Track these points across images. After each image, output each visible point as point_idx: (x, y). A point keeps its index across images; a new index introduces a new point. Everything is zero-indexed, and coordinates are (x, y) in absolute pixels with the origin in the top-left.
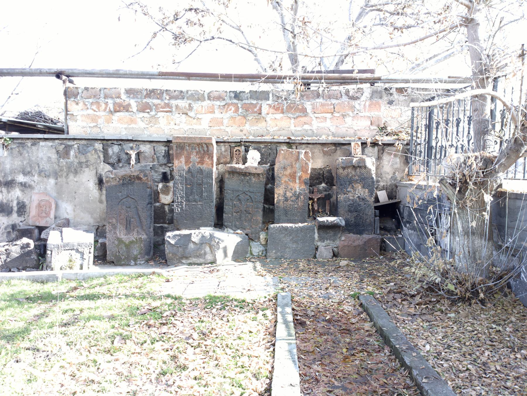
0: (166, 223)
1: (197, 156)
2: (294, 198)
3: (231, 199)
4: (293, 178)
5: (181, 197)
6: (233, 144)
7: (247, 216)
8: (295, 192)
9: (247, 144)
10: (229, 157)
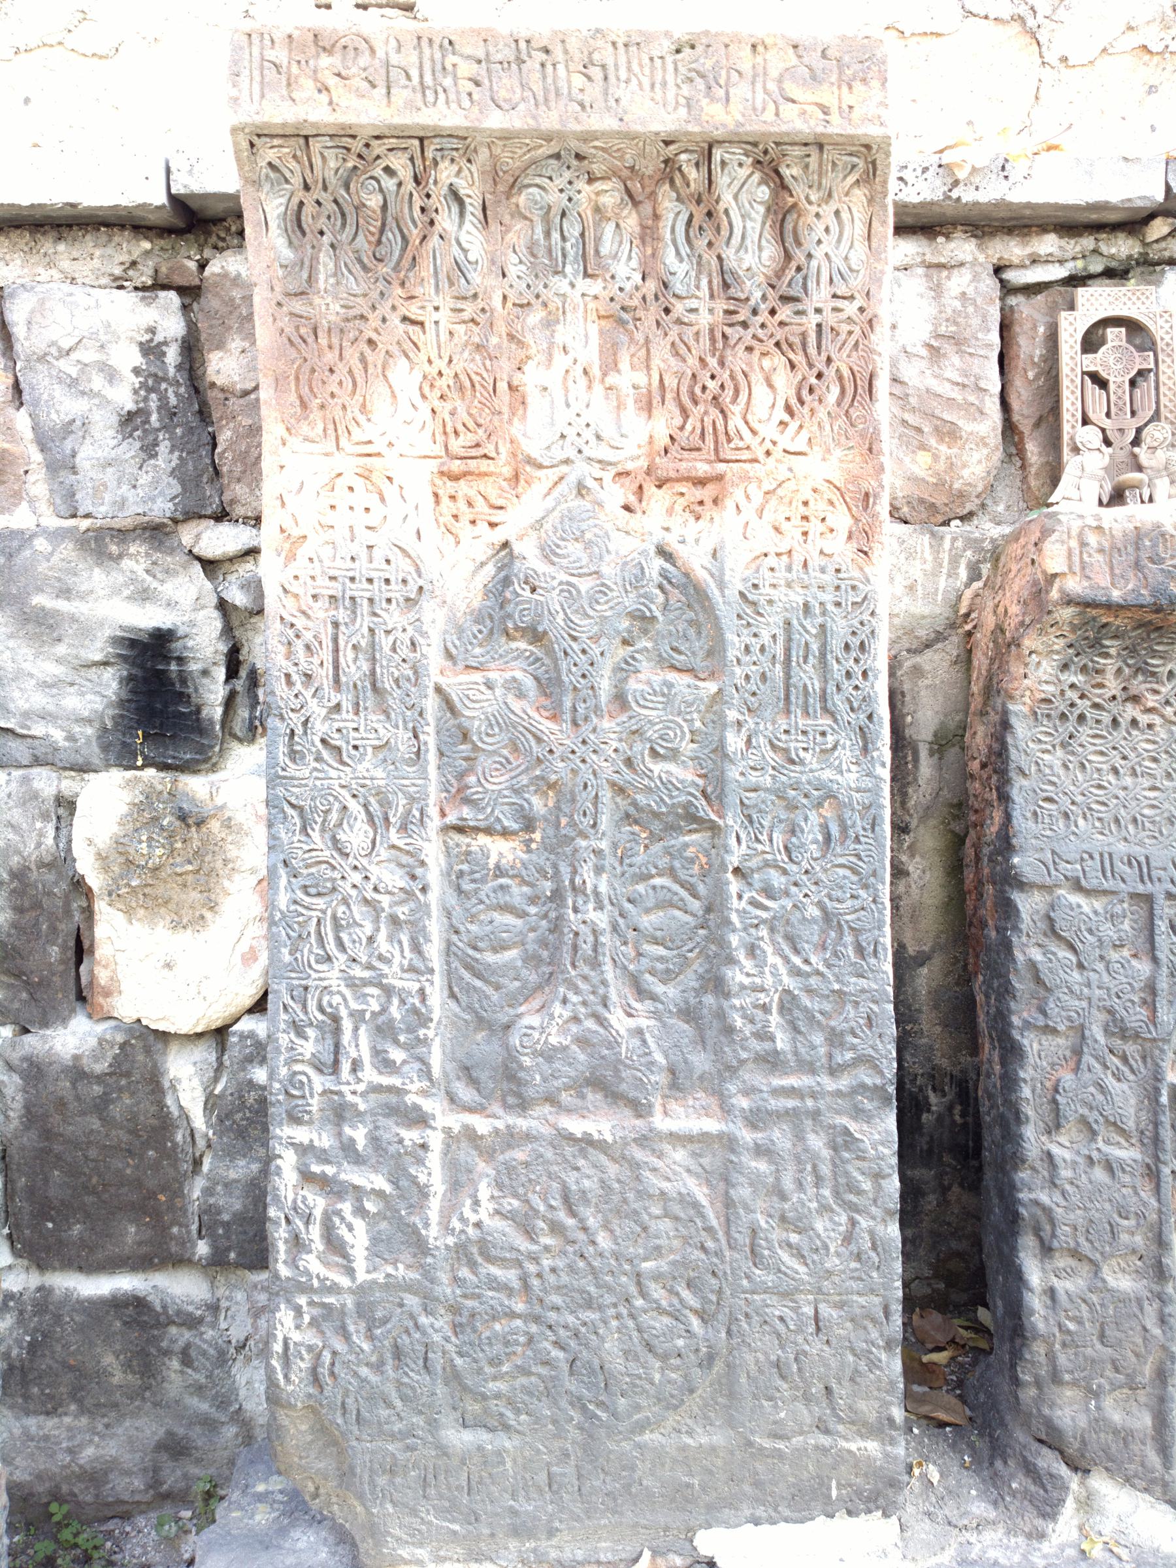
0: (179, 1261)
1: (629, 377)
3: (1118, 1029)
5: (385, 1030)
6: (1049, 244)
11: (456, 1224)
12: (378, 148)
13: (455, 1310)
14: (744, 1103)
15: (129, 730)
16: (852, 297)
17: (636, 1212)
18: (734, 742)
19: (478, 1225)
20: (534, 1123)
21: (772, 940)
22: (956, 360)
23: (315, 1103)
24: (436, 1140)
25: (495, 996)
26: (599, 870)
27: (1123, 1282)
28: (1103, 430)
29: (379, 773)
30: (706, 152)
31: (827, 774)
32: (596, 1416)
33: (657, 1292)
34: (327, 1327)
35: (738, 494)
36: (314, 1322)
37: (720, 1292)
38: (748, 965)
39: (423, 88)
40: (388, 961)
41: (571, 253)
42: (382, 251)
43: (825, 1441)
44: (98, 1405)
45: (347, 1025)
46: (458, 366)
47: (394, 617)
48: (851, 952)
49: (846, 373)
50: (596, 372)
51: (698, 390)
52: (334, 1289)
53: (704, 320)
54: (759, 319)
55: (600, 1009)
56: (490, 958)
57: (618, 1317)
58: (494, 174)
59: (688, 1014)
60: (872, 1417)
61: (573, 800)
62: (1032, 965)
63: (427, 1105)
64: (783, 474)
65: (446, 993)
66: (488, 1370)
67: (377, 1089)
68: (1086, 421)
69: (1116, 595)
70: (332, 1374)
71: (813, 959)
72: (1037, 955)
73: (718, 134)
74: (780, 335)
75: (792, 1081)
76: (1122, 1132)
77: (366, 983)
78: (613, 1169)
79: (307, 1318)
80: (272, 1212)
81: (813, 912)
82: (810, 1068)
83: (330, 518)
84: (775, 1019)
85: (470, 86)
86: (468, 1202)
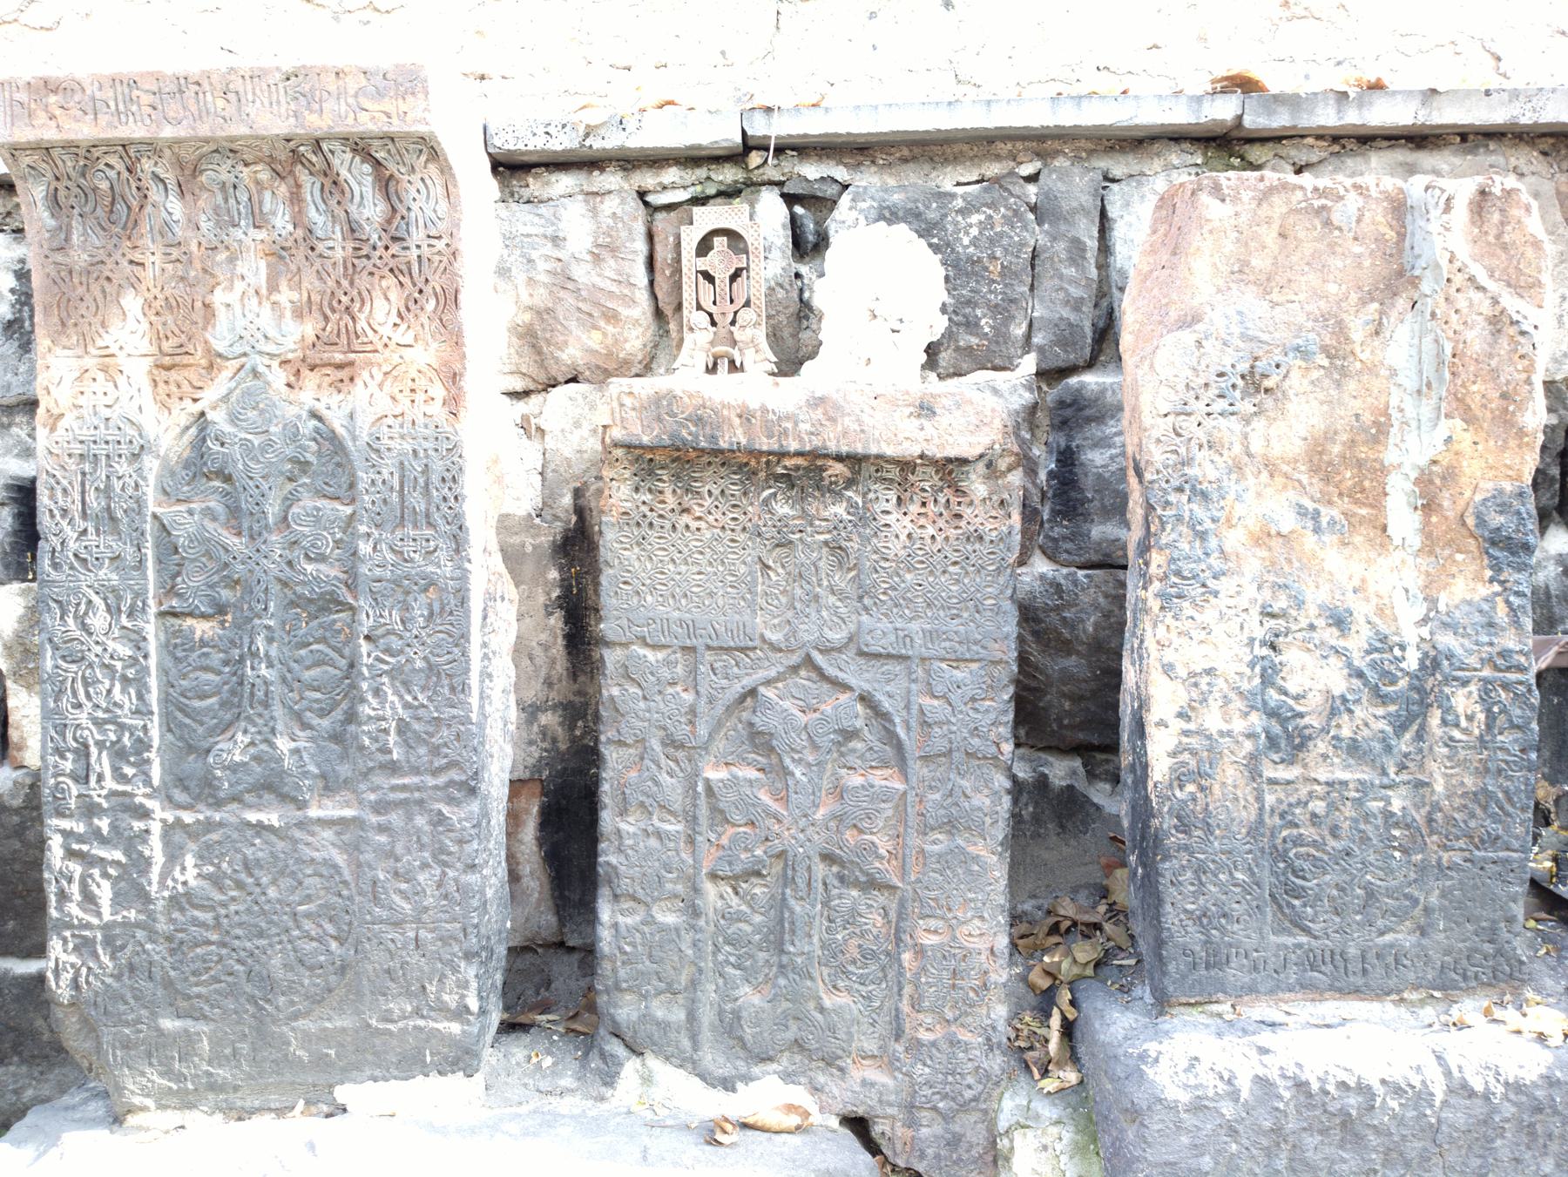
1: (286, 296)
2: (1369, 719)
3: (671, 742)
4: (1357, 494)
5: (119, 754)
6: (671, 175)
7: (852, 917)
8: (1382, 643)
9: (812, 171)
10: (641, 308)
11: (170, 883)
12: (96, 153)
13: (169, 939)
14: (372, 797)
15: (22, 553)
16: (439, 238)
17: (293, 873)
18: (365, 548)
19: (185, 883)
20: (225, 815)
21: (393, 685)
22: (612, 262)
23: (73, 803)
24: (156, 828)
25: (200, 730)
26: (270, 640)
27: (668, 917)
28: (710, 315)
29: (114, 576)
30: (317, 144)
31: (431, 569)
32: (263, 1008)
33: (308, 925)
34: (84, 950)
35: (365, 374)
36: (76, 948)
37: (350, 924)
38: (374, 702)
39: (119, 113)
40: (121, 707)
41: (243, 210)
42: (114, 217)
43: (421, 1023)
44: (33, 1057)
45: (94, 750)
46: (168, 292)
47: (123, 468)
48: (446, 691)
49: (438, 289)
50: (264, 291)
51: (335, 304)
52: (88, 926)
53: (339, 254)
54: (378, 253)
55: (270, 736)
56: (197, 704)
57: (280, 942)
58: (180, 164)
59: (337, 738)
60: (453, 1005)
61: (251, 592)
62: (612, 698)
63: (150, 804)
64: (396, 359)
65: (165, 728)
66: (193, 979)
67: (113, 793)
68: (699, 307)
69: (646, 440)
70: (87, 982)
71: (420, 697)
72: (615, 691)
73: (318, 134)
74: (392, 263)
75: (406, 781)
76: (670, 812)
77: (106, 722)
78: (280, 845)
79: (71, 946)
80: (46, 875)
81: (419, 664)
82: (416, 771)
83: (81, 401)
84: (392, 739)
85: (150, 110)
86: (178, 868)
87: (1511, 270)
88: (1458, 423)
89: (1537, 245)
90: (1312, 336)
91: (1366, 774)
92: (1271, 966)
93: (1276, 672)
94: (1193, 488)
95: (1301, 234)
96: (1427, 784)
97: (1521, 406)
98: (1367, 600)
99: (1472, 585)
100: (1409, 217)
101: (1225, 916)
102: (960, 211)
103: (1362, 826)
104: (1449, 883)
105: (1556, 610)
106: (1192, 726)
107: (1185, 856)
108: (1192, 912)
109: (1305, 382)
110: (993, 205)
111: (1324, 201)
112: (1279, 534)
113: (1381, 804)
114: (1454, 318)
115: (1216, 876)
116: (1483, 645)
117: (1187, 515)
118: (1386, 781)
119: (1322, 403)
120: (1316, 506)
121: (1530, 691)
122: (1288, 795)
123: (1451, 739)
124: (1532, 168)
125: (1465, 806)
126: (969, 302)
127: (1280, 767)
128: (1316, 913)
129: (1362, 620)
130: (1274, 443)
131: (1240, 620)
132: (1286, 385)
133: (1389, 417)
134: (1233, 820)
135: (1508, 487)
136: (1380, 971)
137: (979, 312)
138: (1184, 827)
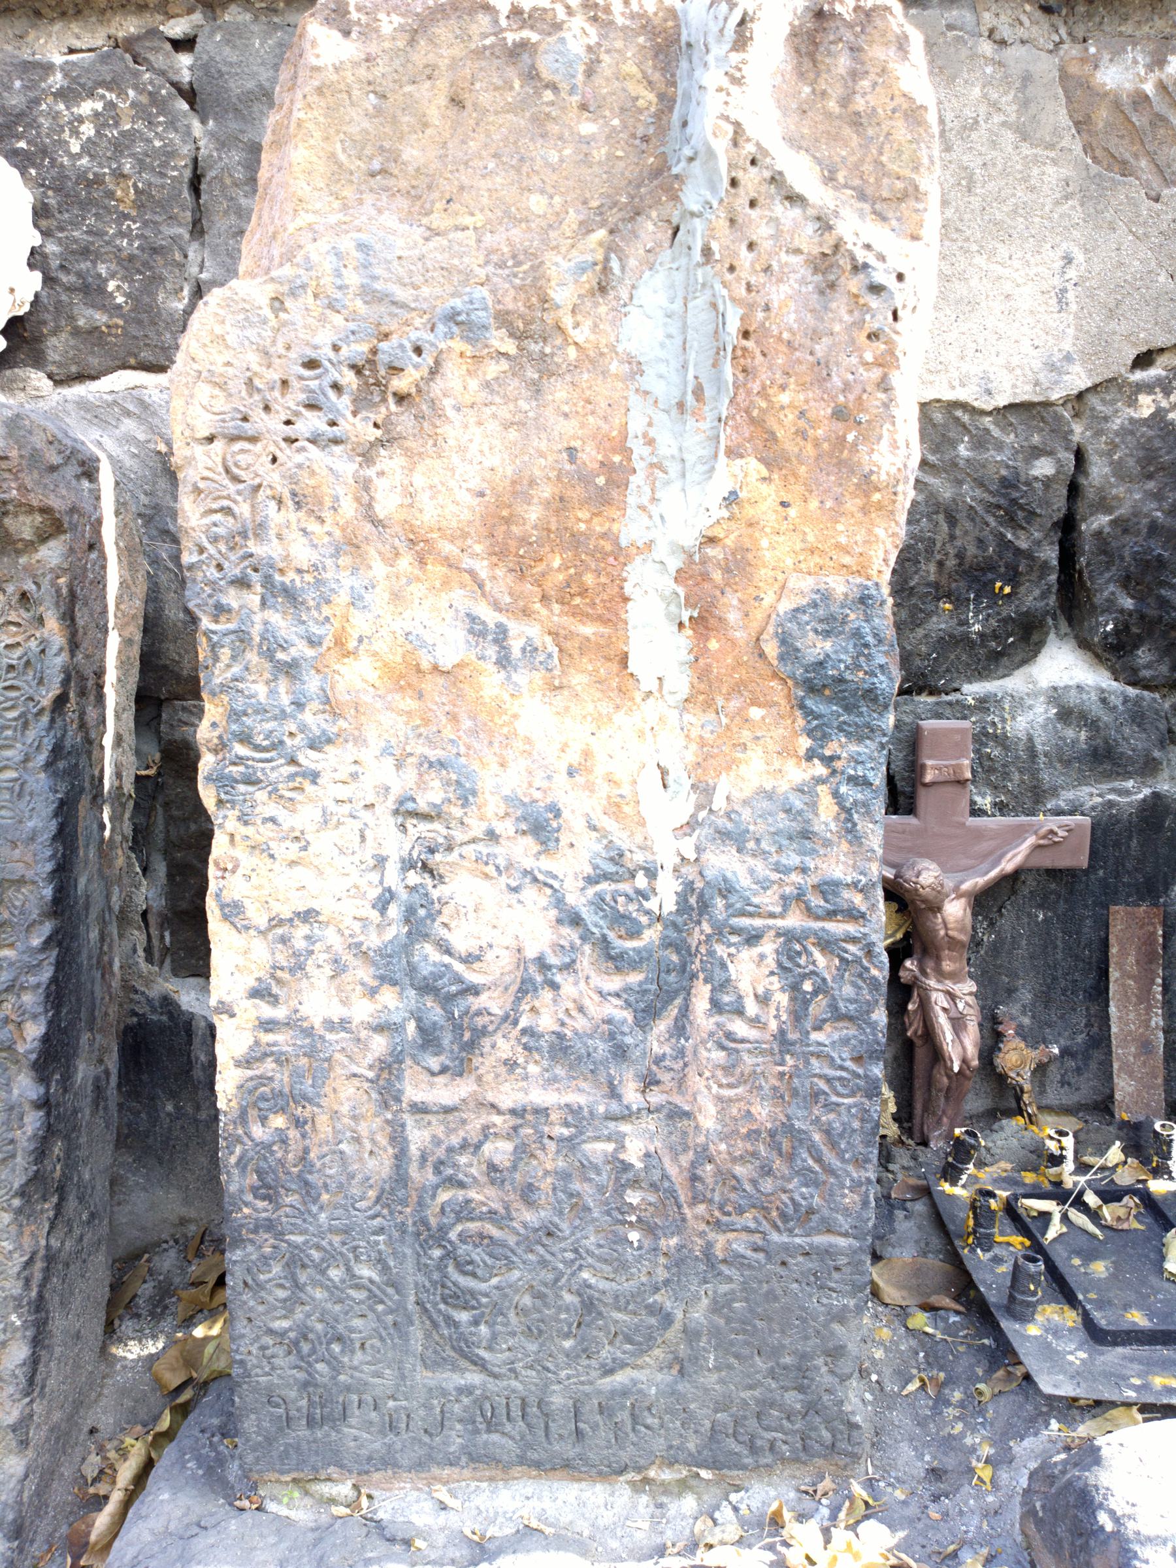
87: (867, 167)
88: (753, 466)
89: (914, 114)
90: (484, 292)
91: (583, 1095)
92: (418, 1423)
93: (432, 917)
94: (268, 581)
95: (485, 98)
96: (687, 1115)
97: (868, 434)
98: (590, 787)
99: (777, 765)
100: (684, 64)
101: (339, 1339)
102: (61, 94)
103: (576, 1186)
104: (724, 1288)
105: (1045, 776)
106: (280, 1013)
107: (267, 1241)
108: (283, 1334)
109: (474, 384)
110: (113, 84)
111: (526, 34)
112: (436, 668)
113: (610, 1147)
114: (745, 257)
115: (323, 1272)
116: (786, 871)
117: (256, 631)
118: (614, 1107)
119: (506, 426)
120: (501, 618)
121: (869, 953)
122: (450, 1131)
123: (729, 1036)
124: (1021, 32)
125: (754, 1154)
126: (85, 252)
127: (441, 1080)
128: (494, 1336)
129: (579, 825)
130: (424, 499)
131: (358, 825)
132: (437, 388)
133: (627, 453)
134: (352, 1176)
135: (839, 586)
136: (604, 1434)
137: (102, 269)
138: (268, 1191)
